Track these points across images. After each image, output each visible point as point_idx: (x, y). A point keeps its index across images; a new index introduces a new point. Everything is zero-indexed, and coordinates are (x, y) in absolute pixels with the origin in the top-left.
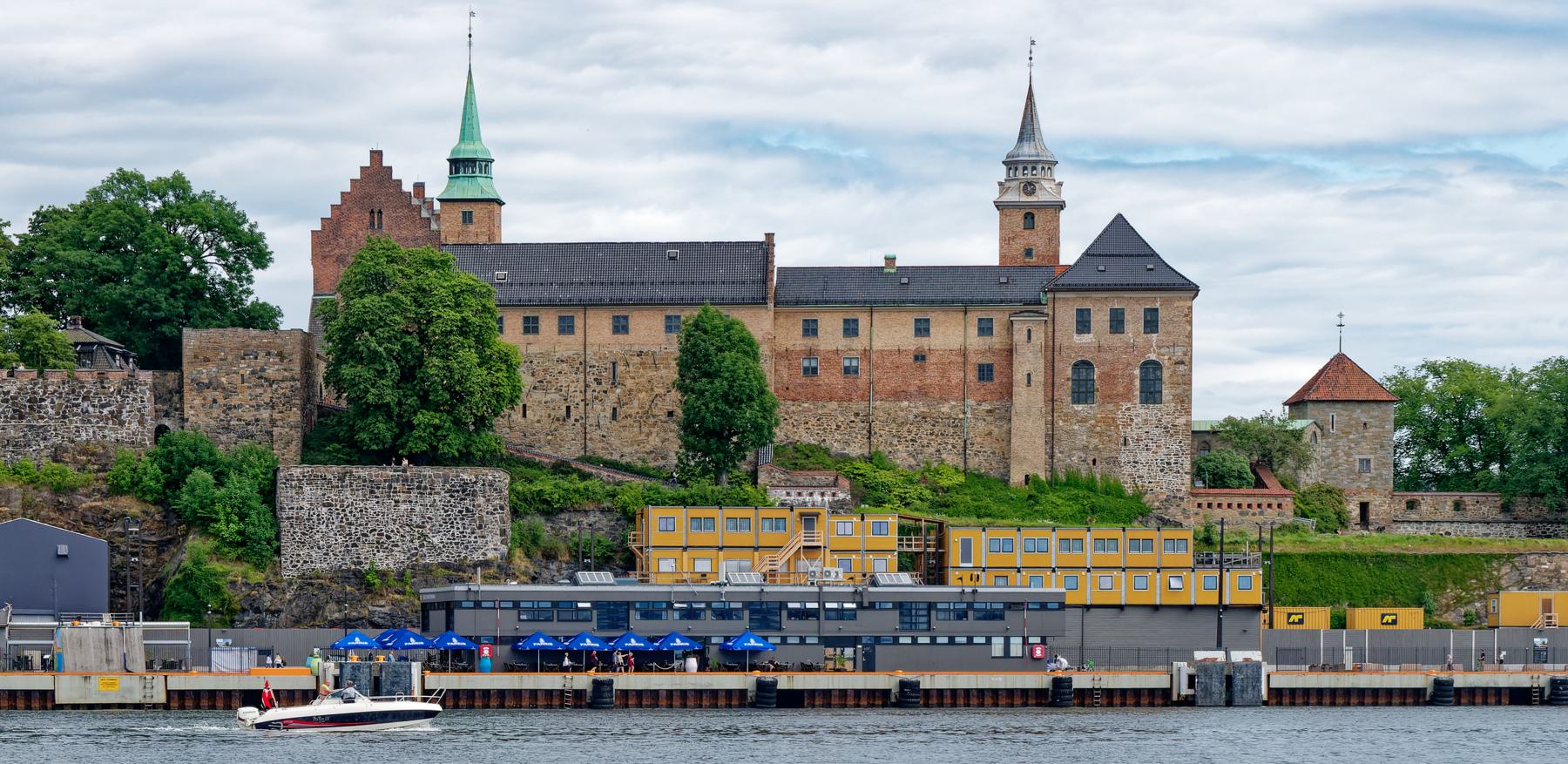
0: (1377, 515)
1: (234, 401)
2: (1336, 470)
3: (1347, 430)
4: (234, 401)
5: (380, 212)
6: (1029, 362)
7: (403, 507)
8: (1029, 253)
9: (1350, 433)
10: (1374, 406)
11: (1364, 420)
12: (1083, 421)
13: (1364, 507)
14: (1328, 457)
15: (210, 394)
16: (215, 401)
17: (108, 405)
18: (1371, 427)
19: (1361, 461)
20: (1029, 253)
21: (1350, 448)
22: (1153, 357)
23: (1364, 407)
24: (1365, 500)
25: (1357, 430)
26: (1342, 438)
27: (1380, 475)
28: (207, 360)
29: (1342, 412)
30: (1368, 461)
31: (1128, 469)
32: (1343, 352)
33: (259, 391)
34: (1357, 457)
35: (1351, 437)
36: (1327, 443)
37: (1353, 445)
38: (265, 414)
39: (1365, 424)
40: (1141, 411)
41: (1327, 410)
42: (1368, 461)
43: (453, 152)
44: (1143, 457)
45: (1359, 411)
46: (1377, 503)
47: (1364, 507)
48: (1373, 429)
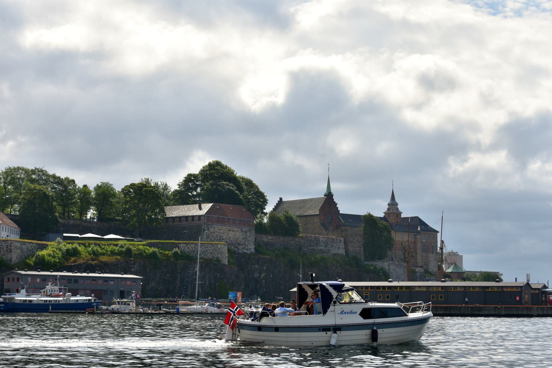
1: (355, 245)
4: (355, 245)
5: (331, 205)
6: (419, 246)
7: (400, 270)
8: (397, 222)
12: (424, 257)
15: (352, 244)
16: (352, 245)
17: (338, 245)
20: (397, 222)
22: (433, 245)
28: (352, 236)
31: (430, 267)
33: (358, 243)
38: (359, 248)
40: (432, 255)
43: (325, 193)
44: (432, 264)
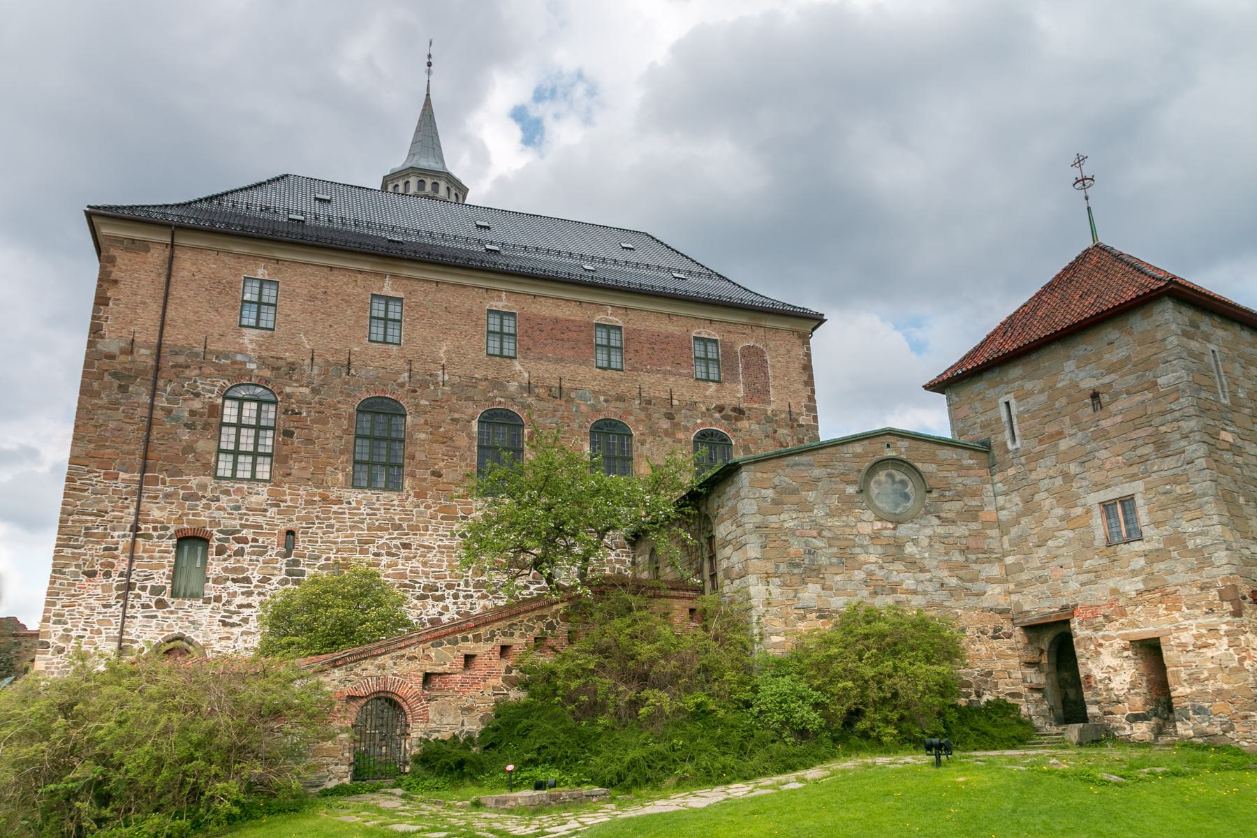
0: (1194, 679)
2: (1042, 552)
3: (1051, 429)
9: (1060, 434)
10: (1110, 333)
11: (1089, 384)
13: (1150, 650)
14: (1016, 521)
18: (1115, 397)
19: (1107, 507)
21: (1067, 477)
23: (1084, 347)
24: (1146, 631)
25: (1076, 423)
26: (1041, 455)
27: (1177, 540)
29: (1029, 385)
30: (1127, 502)
32: (1104, 240)
34: (1094, 499)
35: (1064, 445)
36: (1004, 481)
37: (1073, 468)
39: (1095, 396)
41: (990, 393)
42: (1127, 502)
45: (1070, 365)
46: (1186, 637)
47: (1150, 650)
48: (1123, 403)
